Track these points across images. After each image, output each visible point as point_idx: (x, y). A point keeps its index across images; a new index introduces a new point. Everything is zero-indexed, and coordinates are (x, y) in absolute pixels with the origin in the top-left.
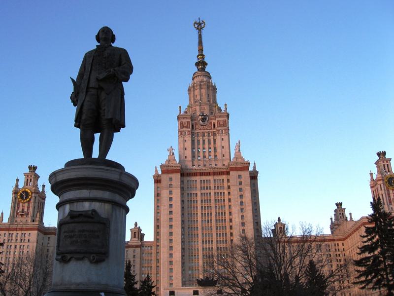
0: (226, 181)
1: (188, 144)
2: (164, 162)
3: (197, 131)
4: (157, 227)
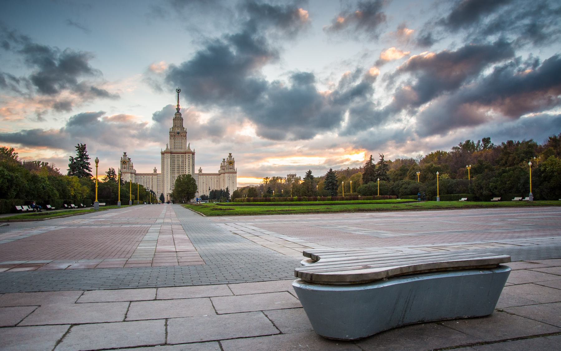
0: (185, 156)
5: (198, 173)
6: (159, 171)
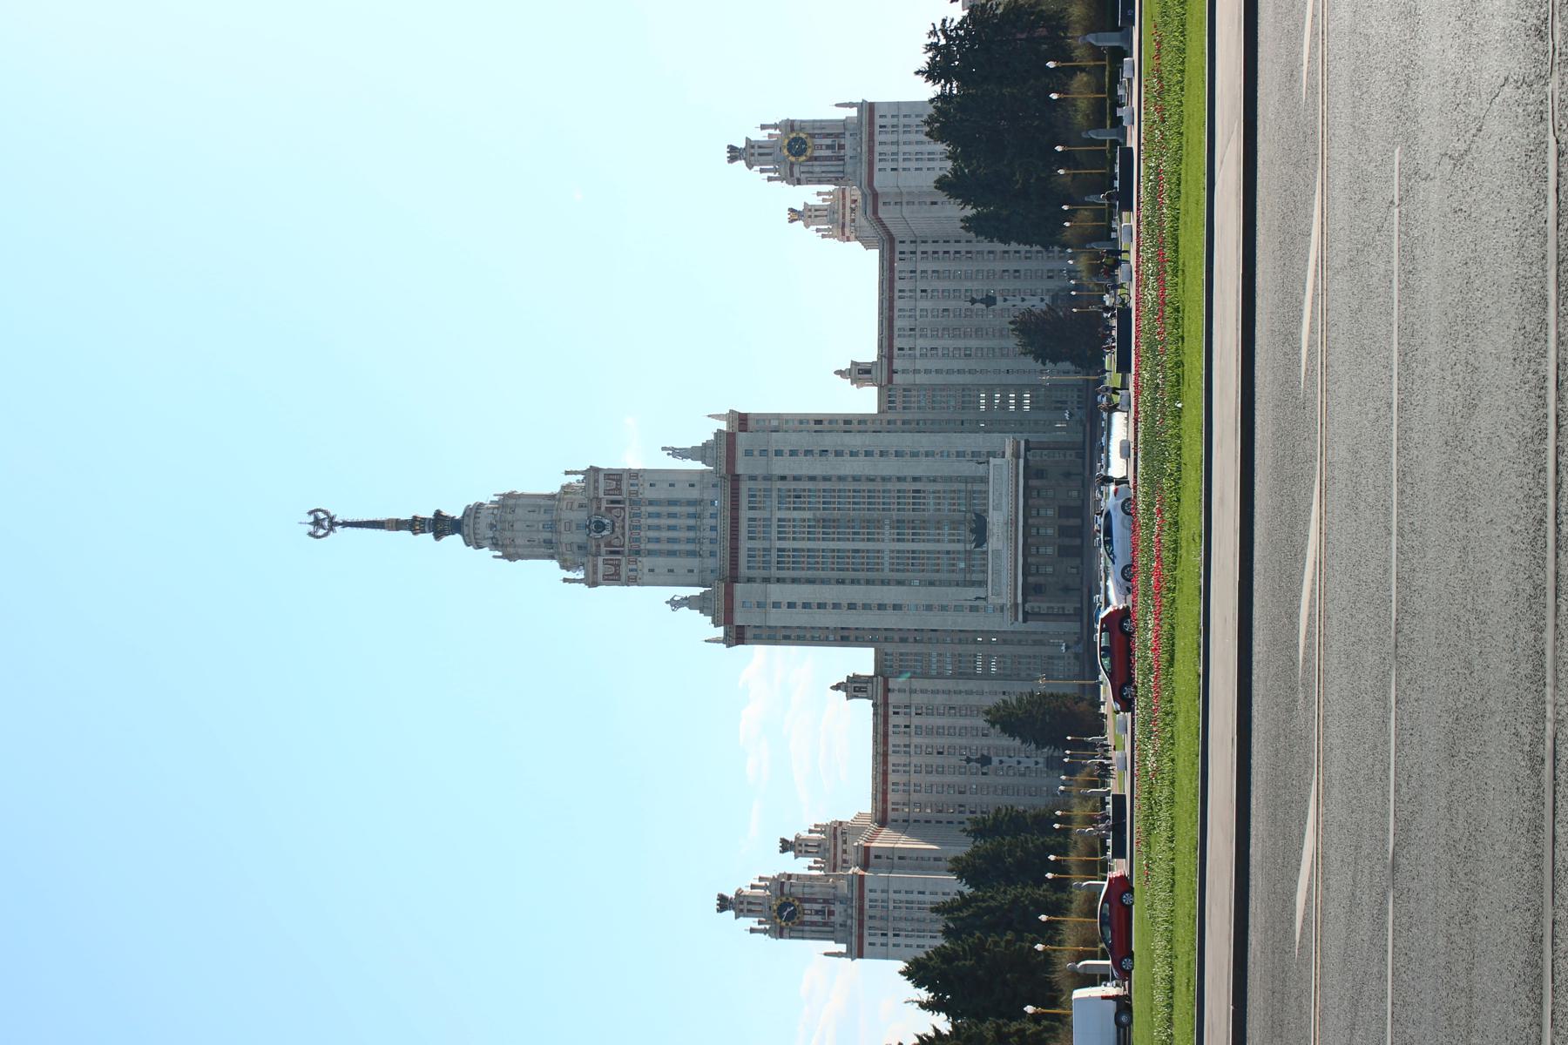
0: (751, 484)
1: (661, 563)
2: (709, 619)
3: (627, 540)
4: (845, 637)
5: (875, 390)
6: (862, 660)
